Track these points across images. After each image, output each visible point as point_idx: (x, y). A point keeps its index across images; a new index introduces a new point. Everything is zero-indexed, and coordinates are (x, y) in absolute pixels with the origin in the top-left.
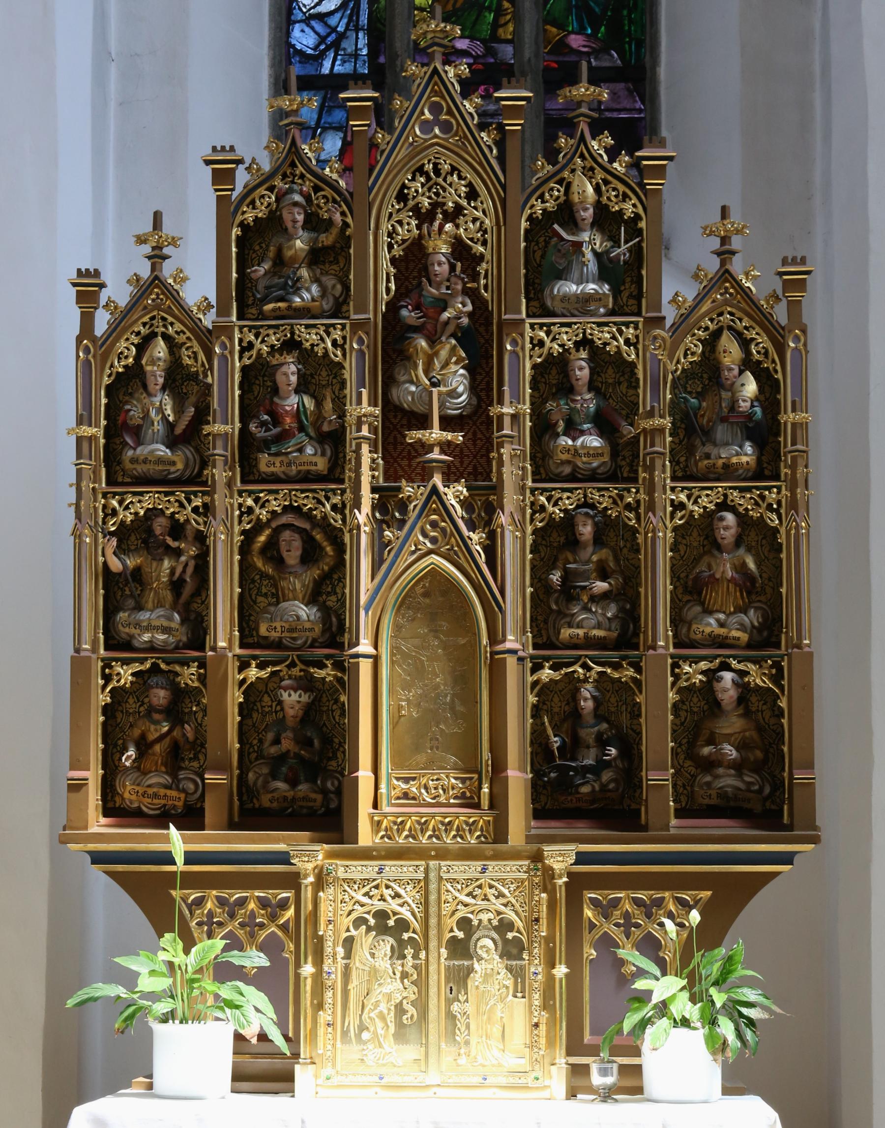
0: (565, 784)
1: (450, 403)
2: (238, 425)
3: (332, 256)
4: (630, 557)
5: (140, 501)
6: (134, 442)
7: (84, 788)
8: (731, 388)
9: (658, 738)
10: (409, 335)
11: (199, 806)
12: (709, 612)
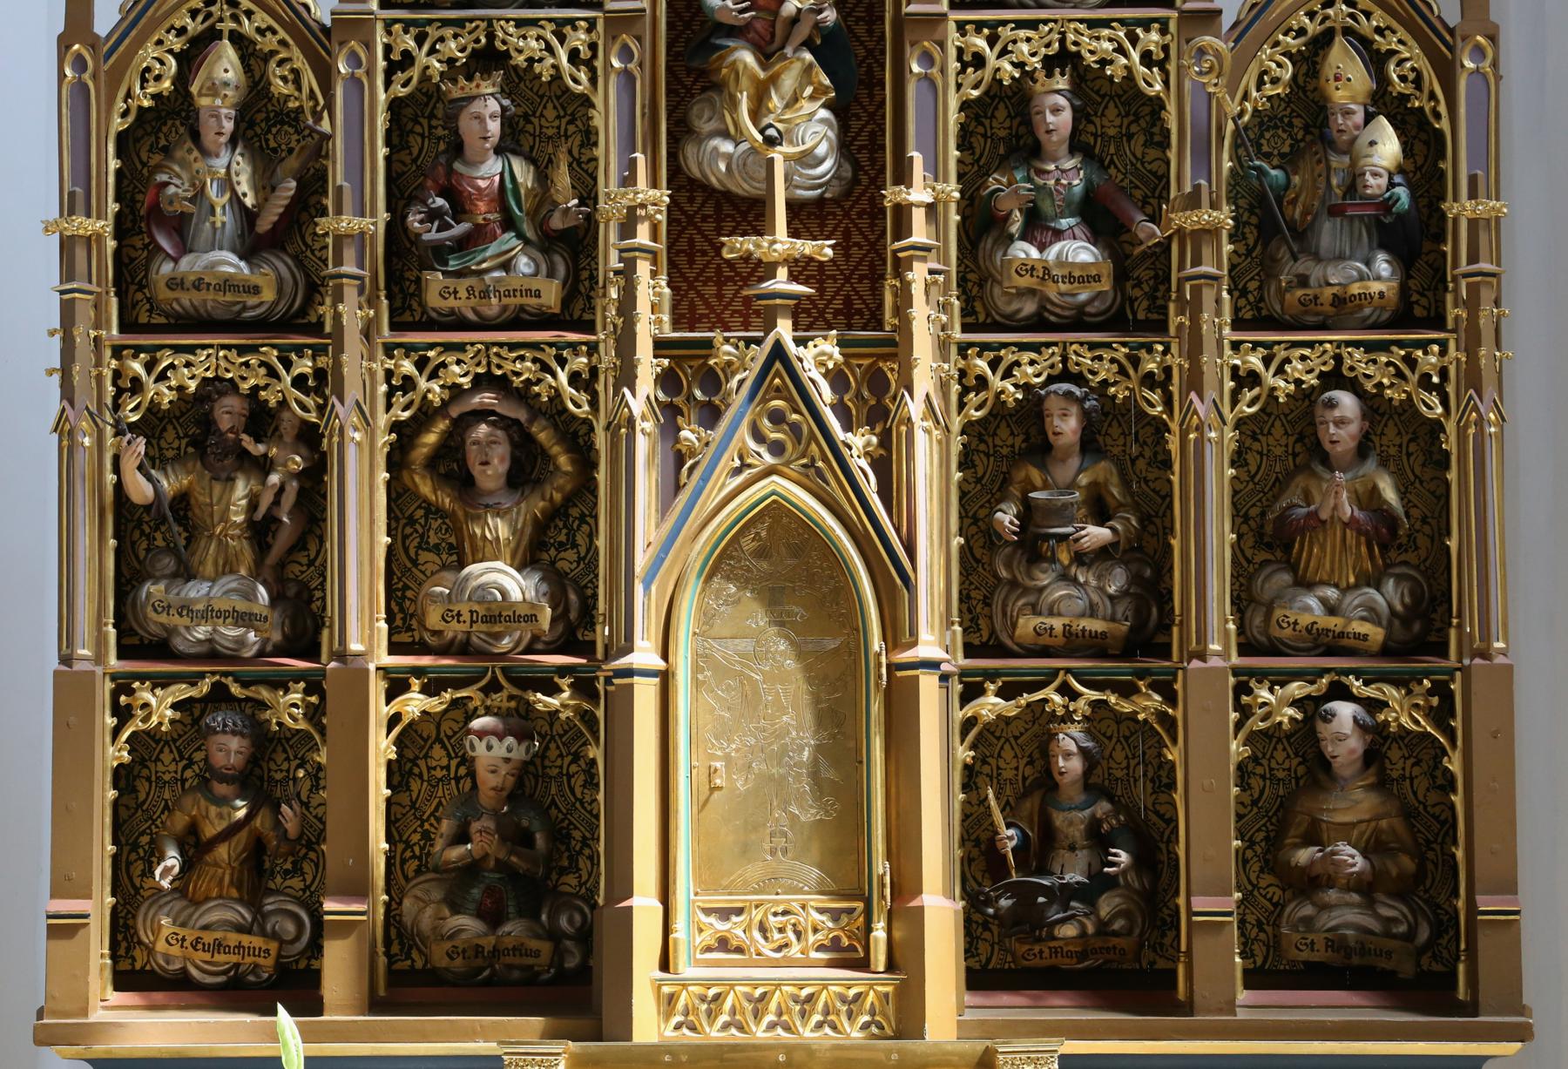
0: (1029, 919)
1: (801, 175)
2: (383, 216)
4: (1151, 476)
5: (188, 365)
6: (175, 246)
7: (81, 932)
8: (1349, 148)
9: (1209, 834)
10: (718, 42)
11: (302, 965)
12: (1305, 583)
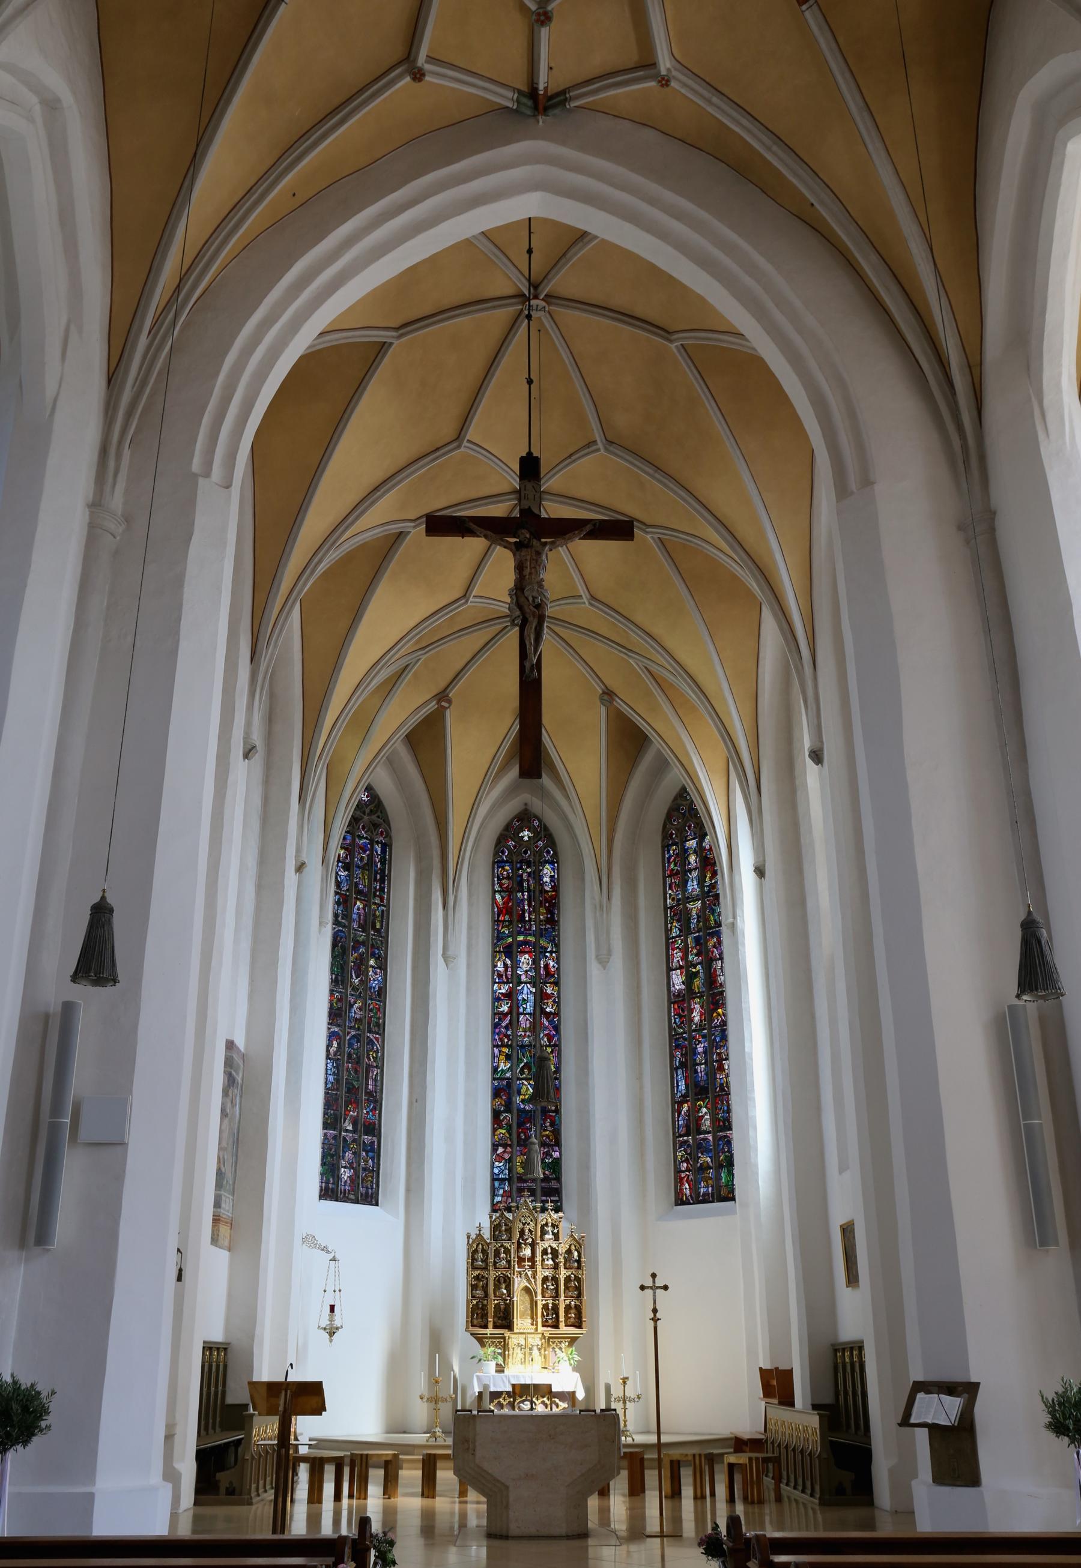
0: (547, 1321)
3: (509, 1231)
